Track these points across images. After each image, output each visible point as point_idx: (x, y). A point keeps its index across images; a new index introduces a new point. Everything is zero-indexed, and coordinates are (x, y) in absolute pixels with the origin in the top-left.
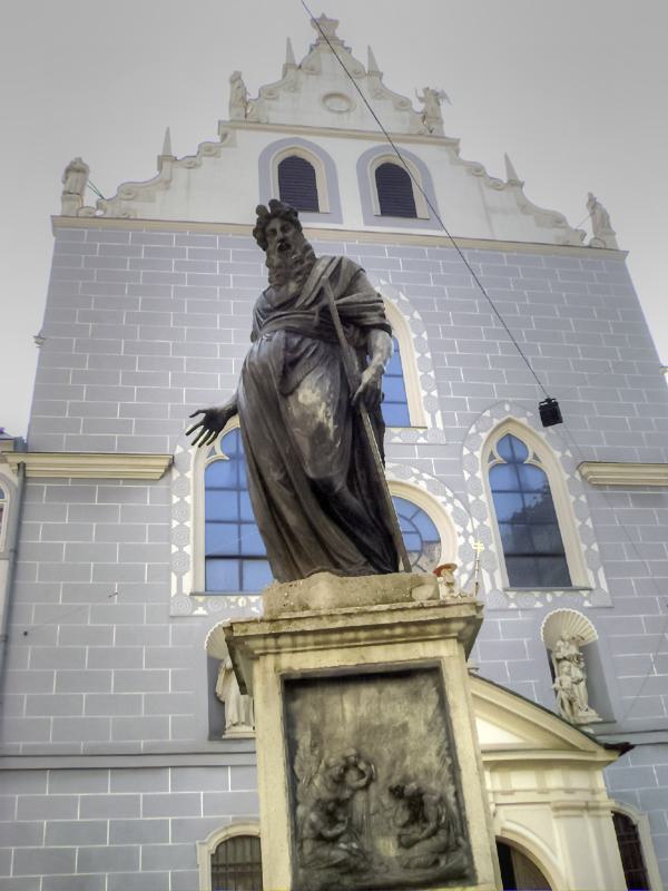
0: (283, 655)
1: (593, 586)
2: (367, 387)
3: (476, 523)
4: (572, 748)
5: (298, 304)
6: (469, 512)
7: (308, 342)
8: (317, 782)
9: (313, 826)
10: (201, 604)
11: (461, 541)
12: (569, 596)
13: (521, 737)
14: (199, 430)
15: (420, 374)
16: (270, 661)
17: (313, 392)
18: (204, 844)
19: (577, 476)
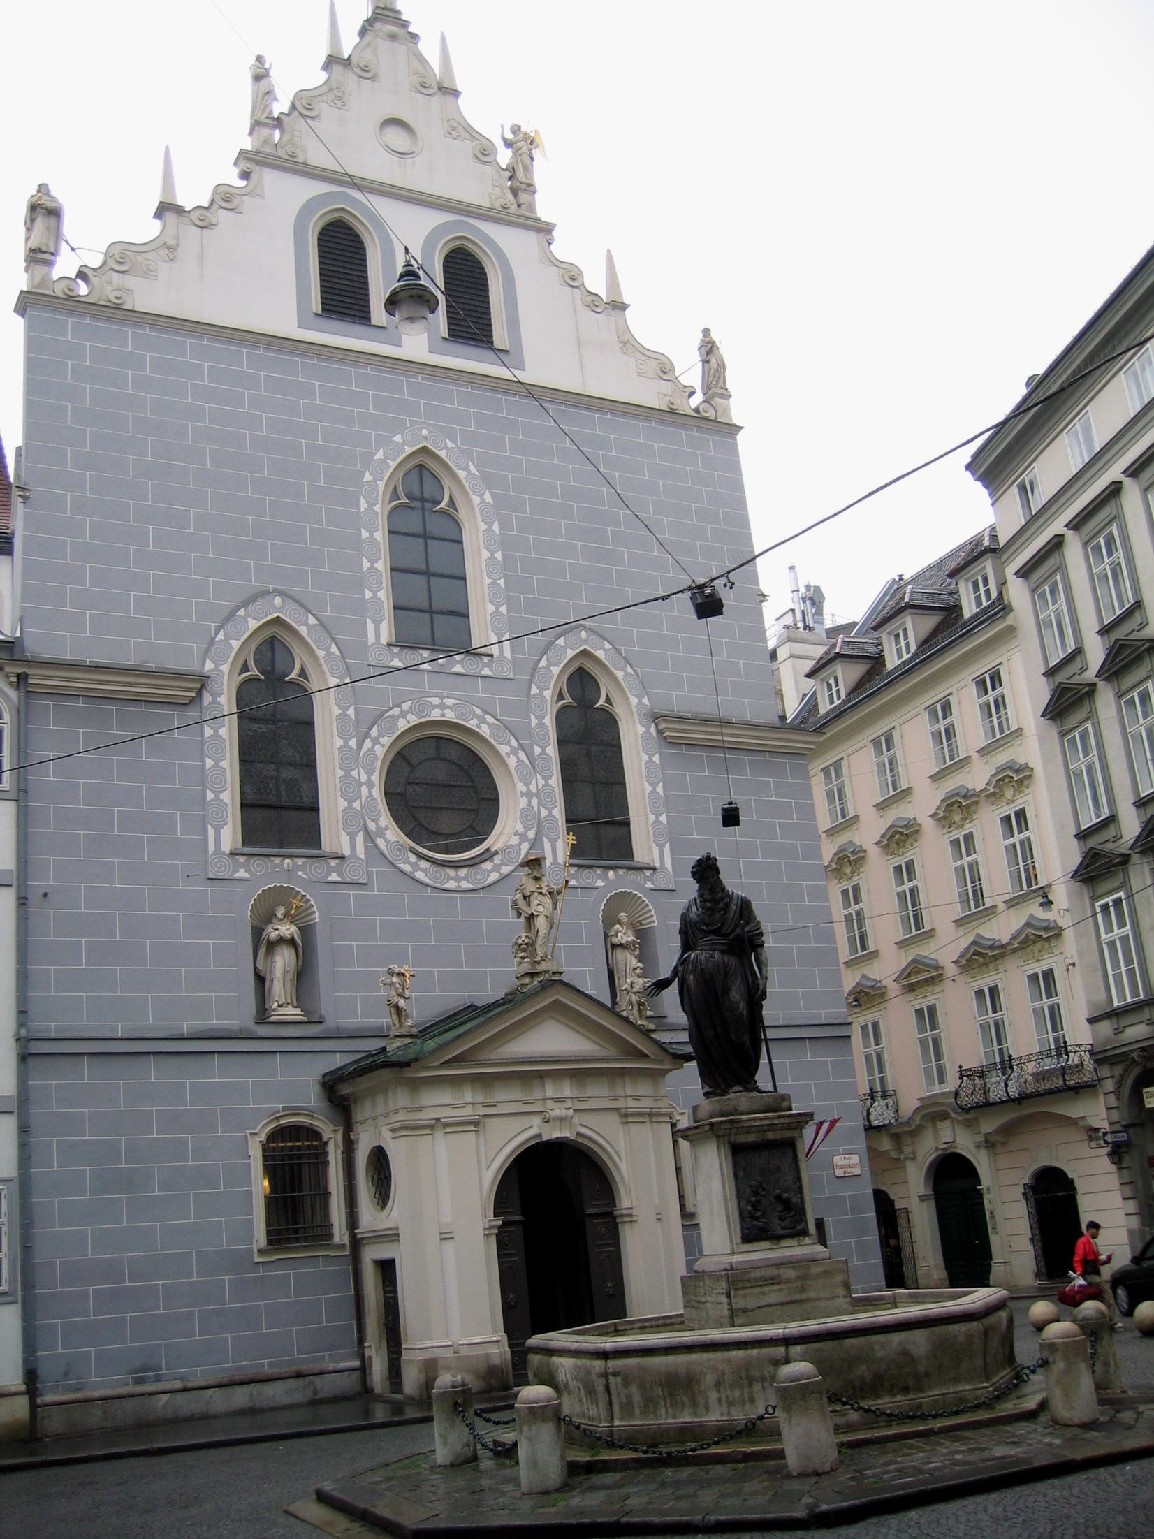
1: (657, 865)
3: (541, 782)
4: (642, 1056)
6: (533, 767)
10: (242, 866)
11: (523, 802)
12: (632, 876)
13: (597, 1044)
15: (488, 581)
16: (726, 1138)
18: (255, 1134)
19: (653, 729)
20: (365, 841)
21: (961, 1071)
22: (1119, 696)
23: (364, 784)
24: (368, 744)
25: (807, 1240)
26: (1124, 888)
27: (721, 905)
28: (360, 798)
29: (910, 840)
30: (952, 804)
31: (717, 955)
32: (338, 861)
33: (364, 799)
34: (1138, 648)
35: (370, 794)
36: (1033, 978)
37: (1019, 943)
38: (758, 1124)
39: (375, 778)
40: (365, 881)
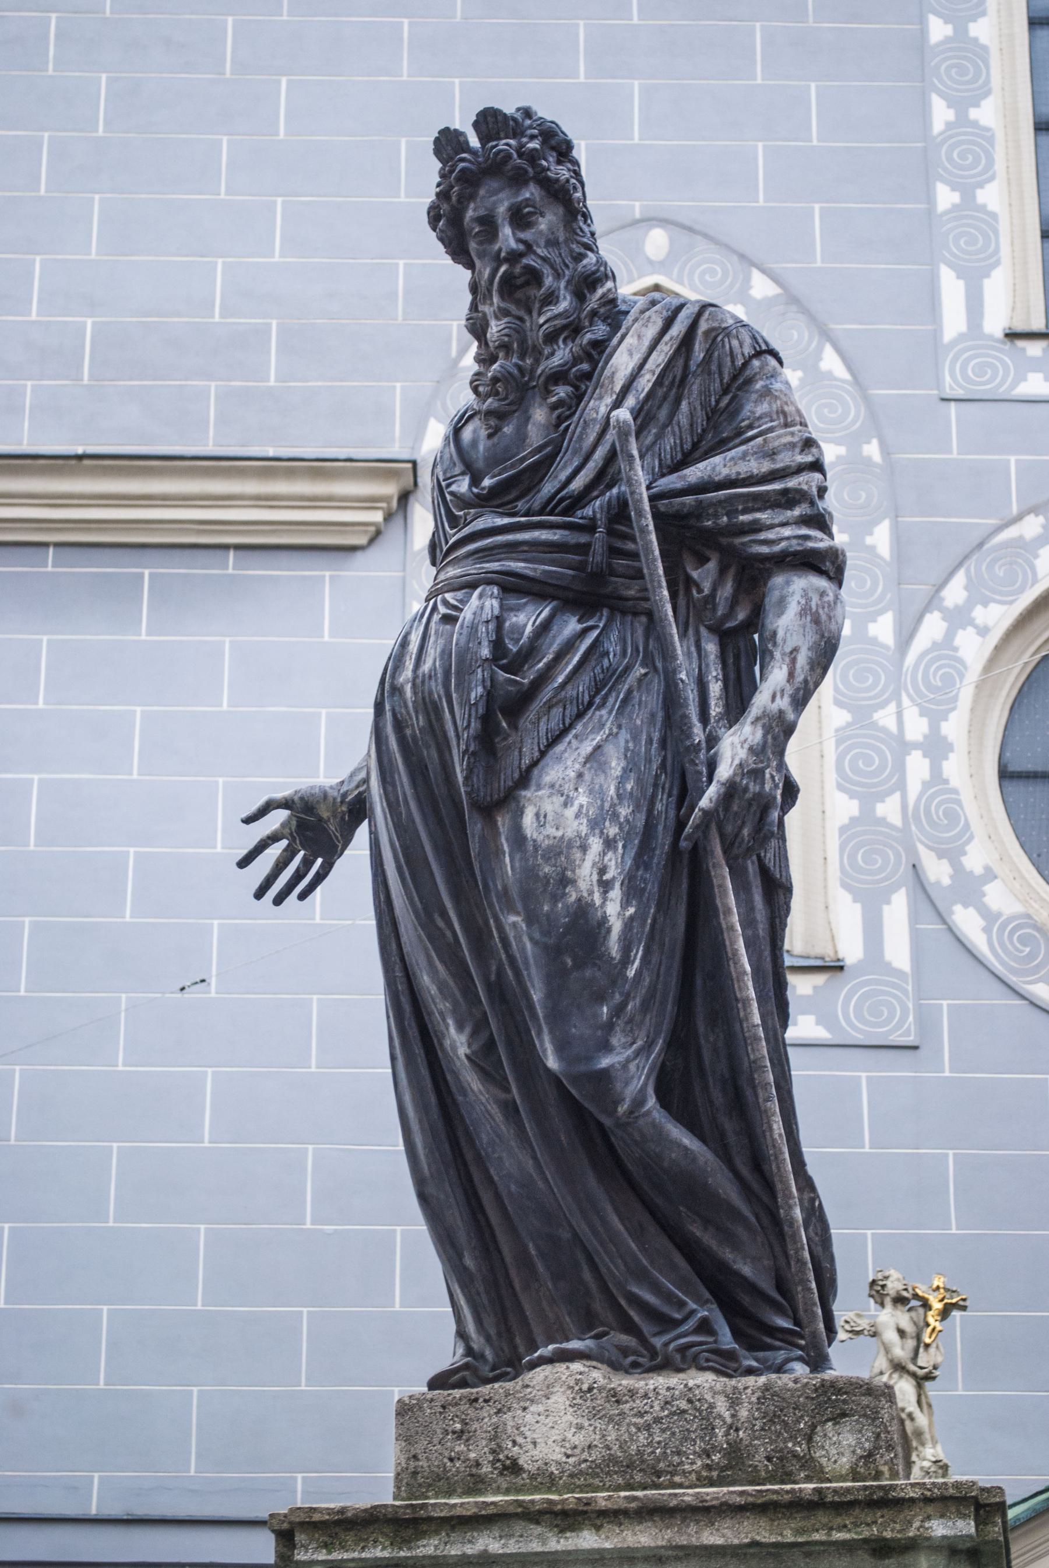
2: (731, 791)
5: (548, 488)
7: (572, 625)
14: (275, 851)
20: (914, 918)
23: (916, 746)
24: (933, 627)
28: (901, 786)
32: (820, 979)
33: (914, 788)
35: (937, 776)
39: (954, 727)
40: (910, 1040)
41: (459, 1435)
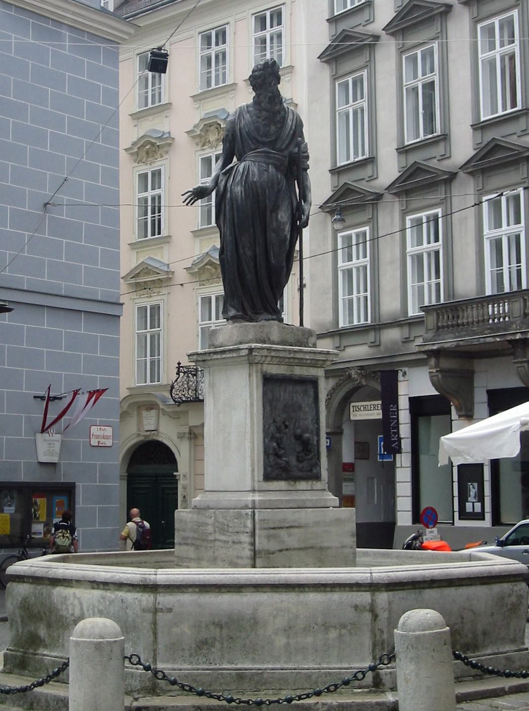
0: (264, 365)
8: (272, 428)
9: (274, 449)
16: (259, 366)
17: (285, 215)
21: (179, 368)
22: (401, 51)
25: (318, 485)
26: (371, 224)
27: (278, 118)
29: (161, 151)
30: (210, 125)
31: (271, 169)
34: (432, 10)
36: (142, 310)
37: (198, 269)
38: (292, 355)
41: (262, 332)
